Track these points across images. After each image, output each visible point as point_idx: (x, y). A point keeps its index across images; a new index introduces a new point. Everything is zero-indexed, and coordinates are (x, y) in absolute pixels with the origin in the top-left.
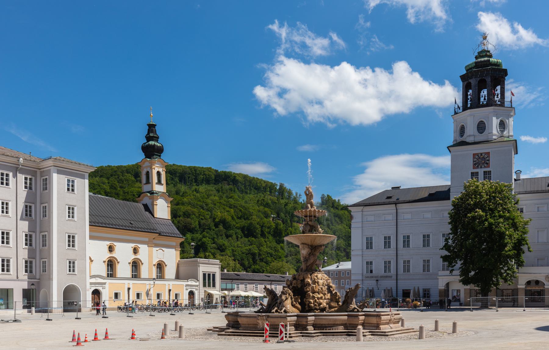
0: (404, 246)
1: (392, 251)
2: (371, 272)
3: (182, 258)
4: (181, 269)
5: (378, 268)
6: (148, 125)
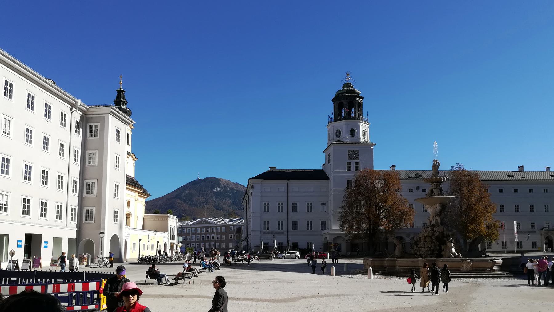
0: (293, 211)
1: (284, 214)
2: (268, 229)
3: (146, 212)
4: (146, 223)
5: (273, 227)
6: (117, 91)
